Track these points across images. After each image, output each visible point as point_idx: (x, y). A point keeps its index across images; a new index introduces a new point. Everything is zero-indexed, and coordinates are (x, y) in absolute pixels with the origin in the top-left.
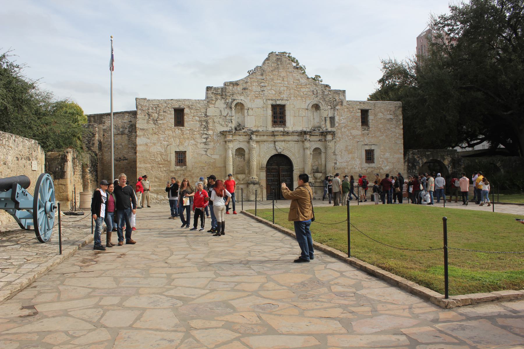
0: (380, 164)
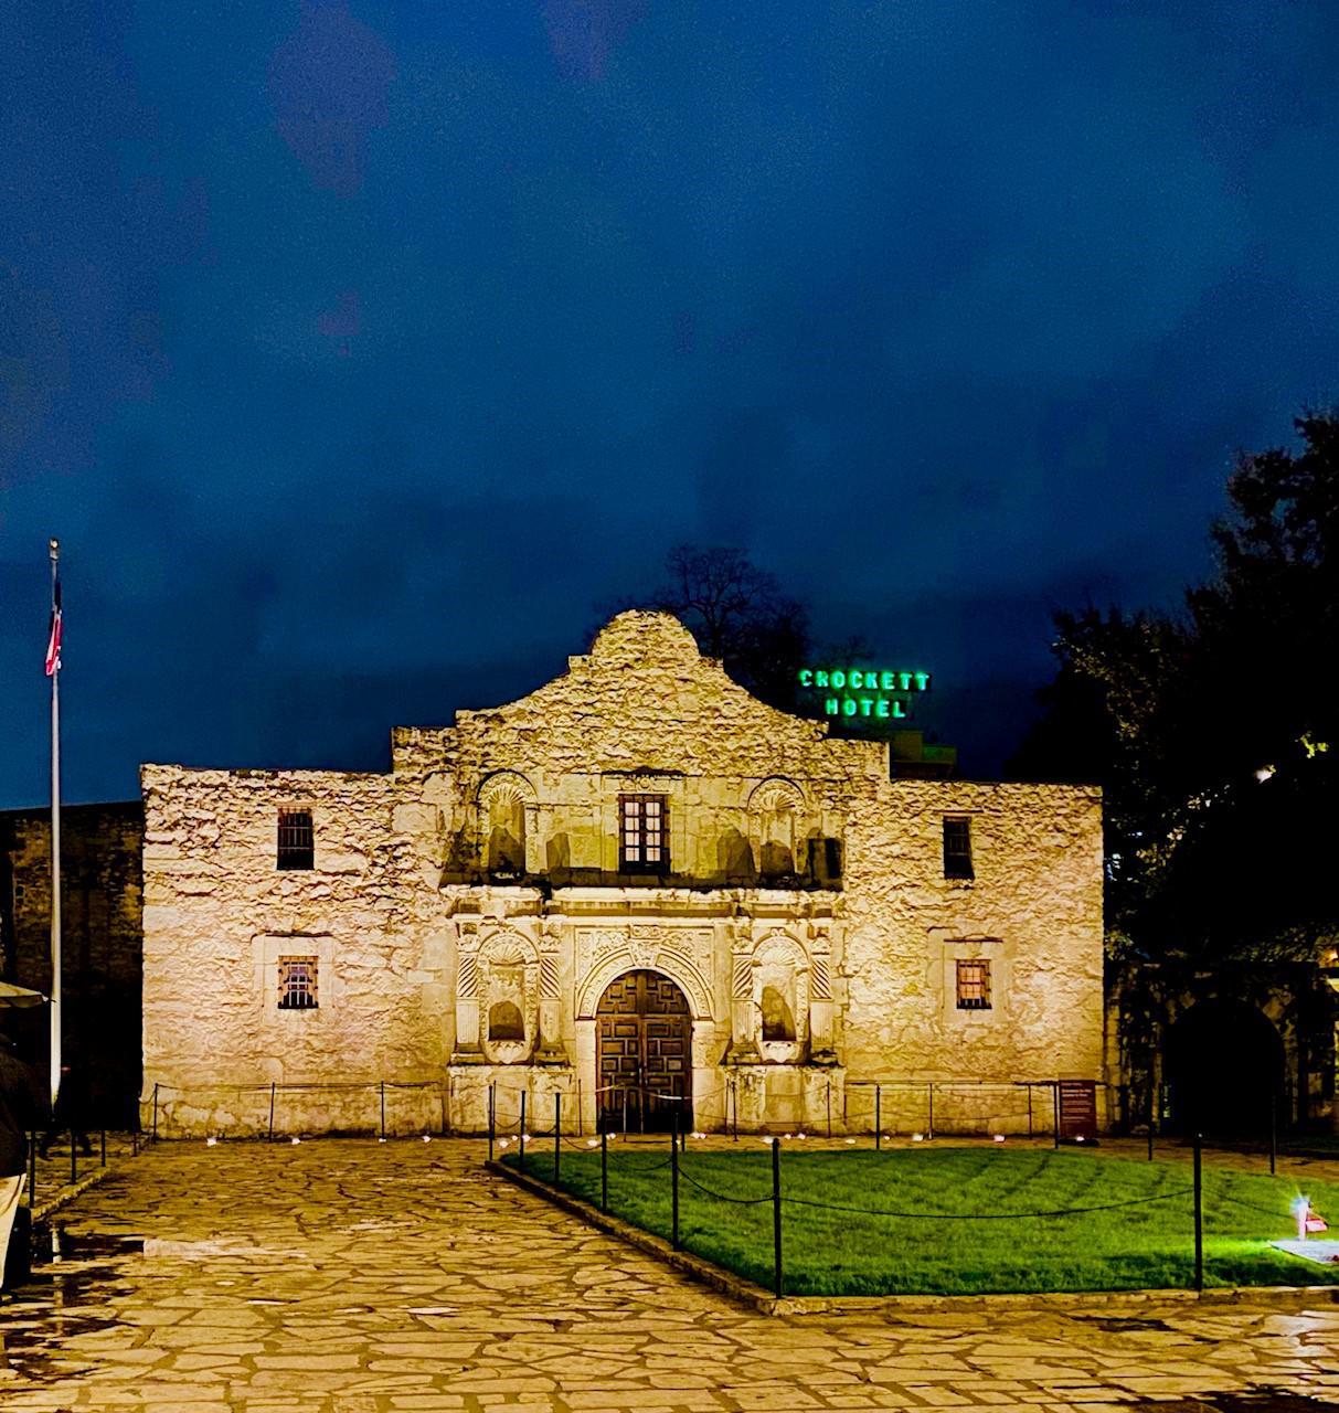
0: (1011, 1013)
